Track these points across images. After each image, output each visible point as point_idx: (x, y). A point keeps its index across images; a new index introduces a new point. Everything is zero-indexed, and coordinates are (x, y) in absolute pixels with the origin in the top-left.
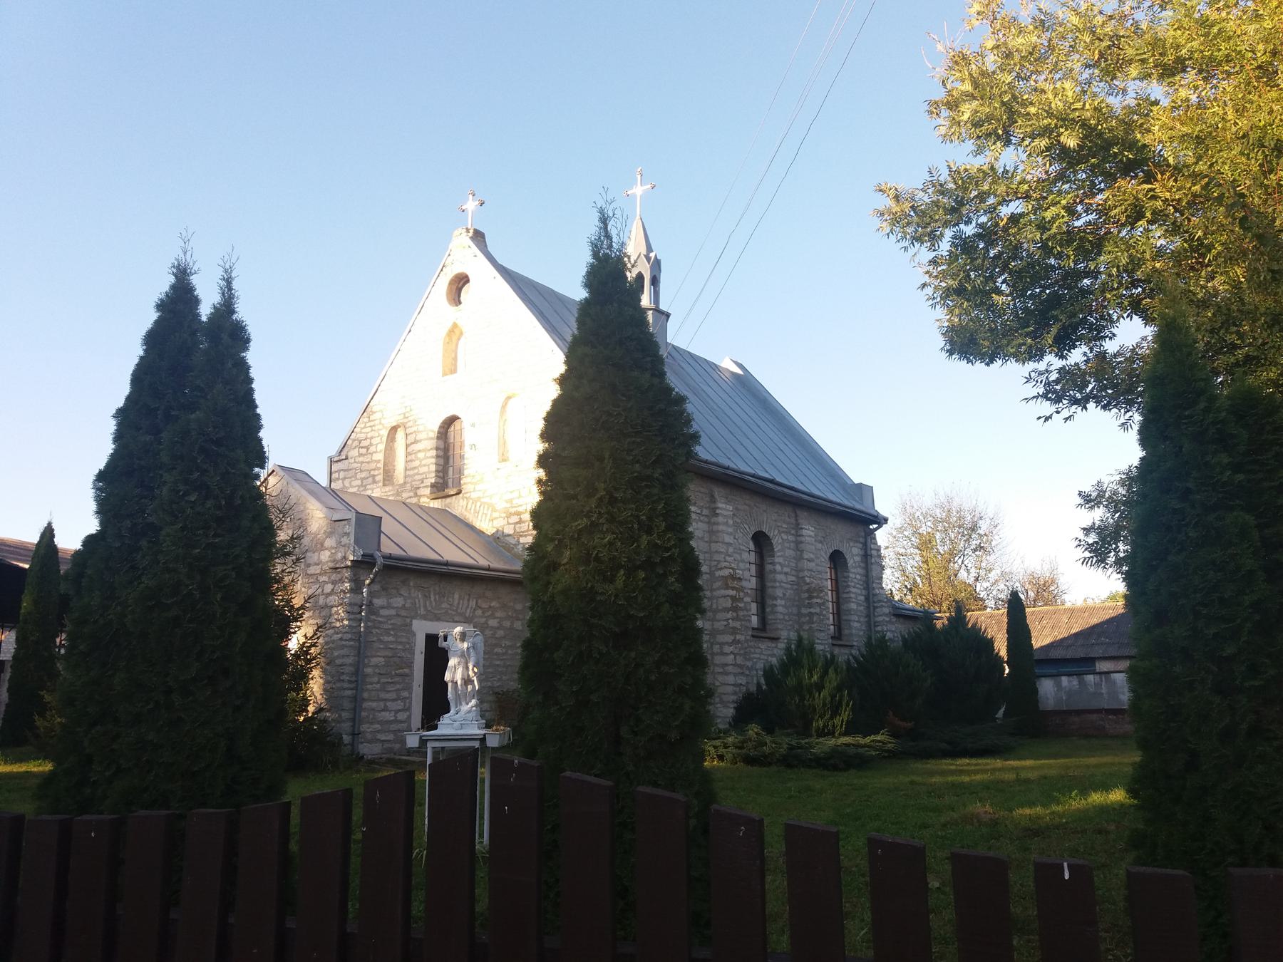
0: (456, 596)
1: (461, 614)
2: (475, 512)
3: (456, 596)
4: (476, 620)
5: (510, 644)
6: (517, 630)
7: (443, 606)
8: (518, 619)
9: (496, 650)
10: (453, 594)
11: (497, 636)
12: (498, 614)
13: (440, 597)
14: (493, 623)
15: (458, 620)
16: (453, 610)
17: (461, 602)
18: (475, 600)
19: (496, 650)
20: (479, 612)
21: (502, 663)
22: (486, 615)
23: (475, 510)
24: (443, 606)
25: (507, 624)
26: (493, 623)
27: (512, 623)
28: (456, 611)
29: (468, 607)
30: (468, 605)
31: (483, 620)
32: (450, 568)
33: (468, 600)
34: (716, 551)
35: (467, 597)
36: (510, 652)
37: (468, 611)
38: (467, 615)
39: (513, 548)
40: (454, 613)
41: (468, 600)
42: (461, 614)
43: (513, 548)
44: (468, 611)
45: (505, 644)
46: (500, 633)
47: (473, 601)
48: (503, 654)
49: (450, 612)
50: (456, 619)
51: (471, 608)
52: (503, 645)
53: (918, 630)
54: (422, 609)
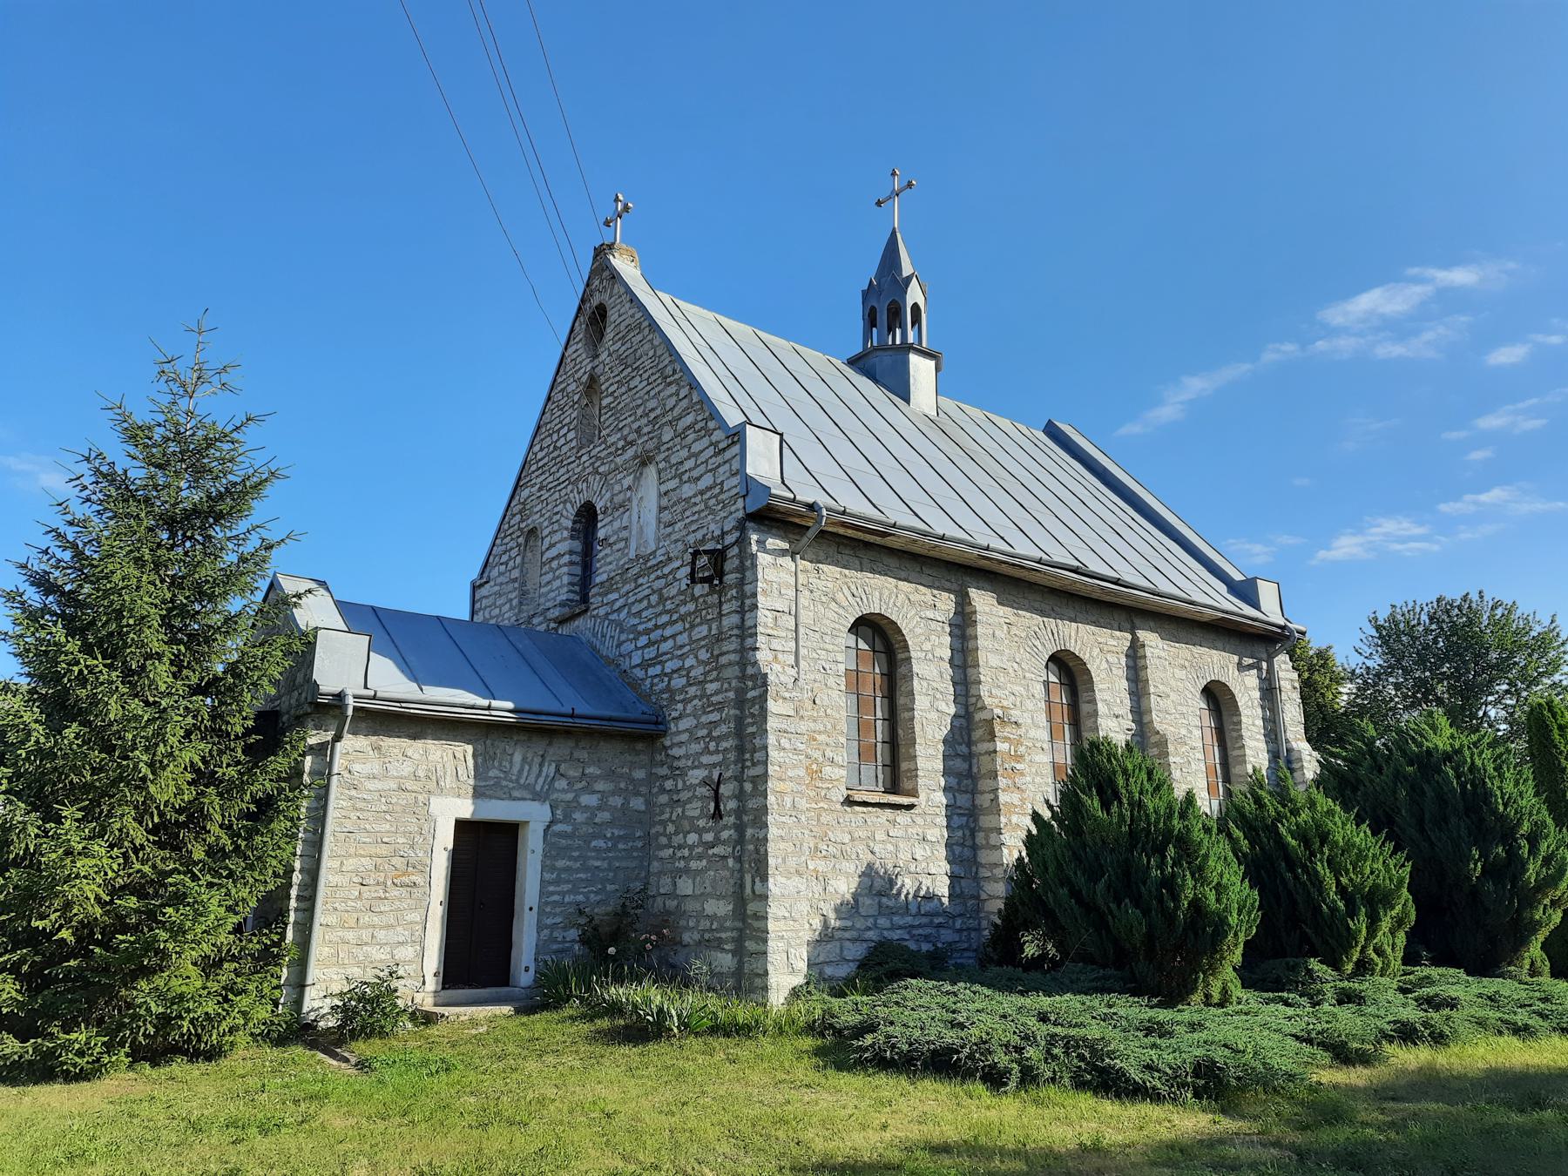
0: (518, 758)
1: (526, 787)
2: (602, 636)
3: (518, 758)
4: (555, 796)
5: (622, 833)
6: (639, 812)
7: (491, 774)
8: (637, 794)
9: (594, 843)
10: (512, 755)
11: (596, 820)
12: (600, 786)
13: (485, 761)
14: (588, 800)
15: (519, 796)
16: (511, 781)
17: (527, 767)
18: (554, 765)
19: (594, 843)
20: (561, 784)
21: (605, 865)
22: (575, 788)
23: (602, 632)
24: (491, 774)
25: (617, 801)
26: (588, 800)
27: (627, 801)
28: (517, 781)
29: (539, 775)
30: (541, 771)
31: (570, 796)
32: (494, 713)
33: (541, 765)
34: (750, 648)
35: (537, 760)
36: (621, 846)
37: (541, 780)
38: (538, 788)
39: (640, 685)
40: (511, 785)
41: (541, 765)
42: (526, 787)
43: (640, 685)
44: (541, 780)
45: (613, 833)
46: (604, 816)
47: (550, 765)
48: (609, 850)
49: (504, 783)
50: (516, 794)
51: (547, 776)
52: (609, 835)
53: (899, 883)
54: (448, 780)
